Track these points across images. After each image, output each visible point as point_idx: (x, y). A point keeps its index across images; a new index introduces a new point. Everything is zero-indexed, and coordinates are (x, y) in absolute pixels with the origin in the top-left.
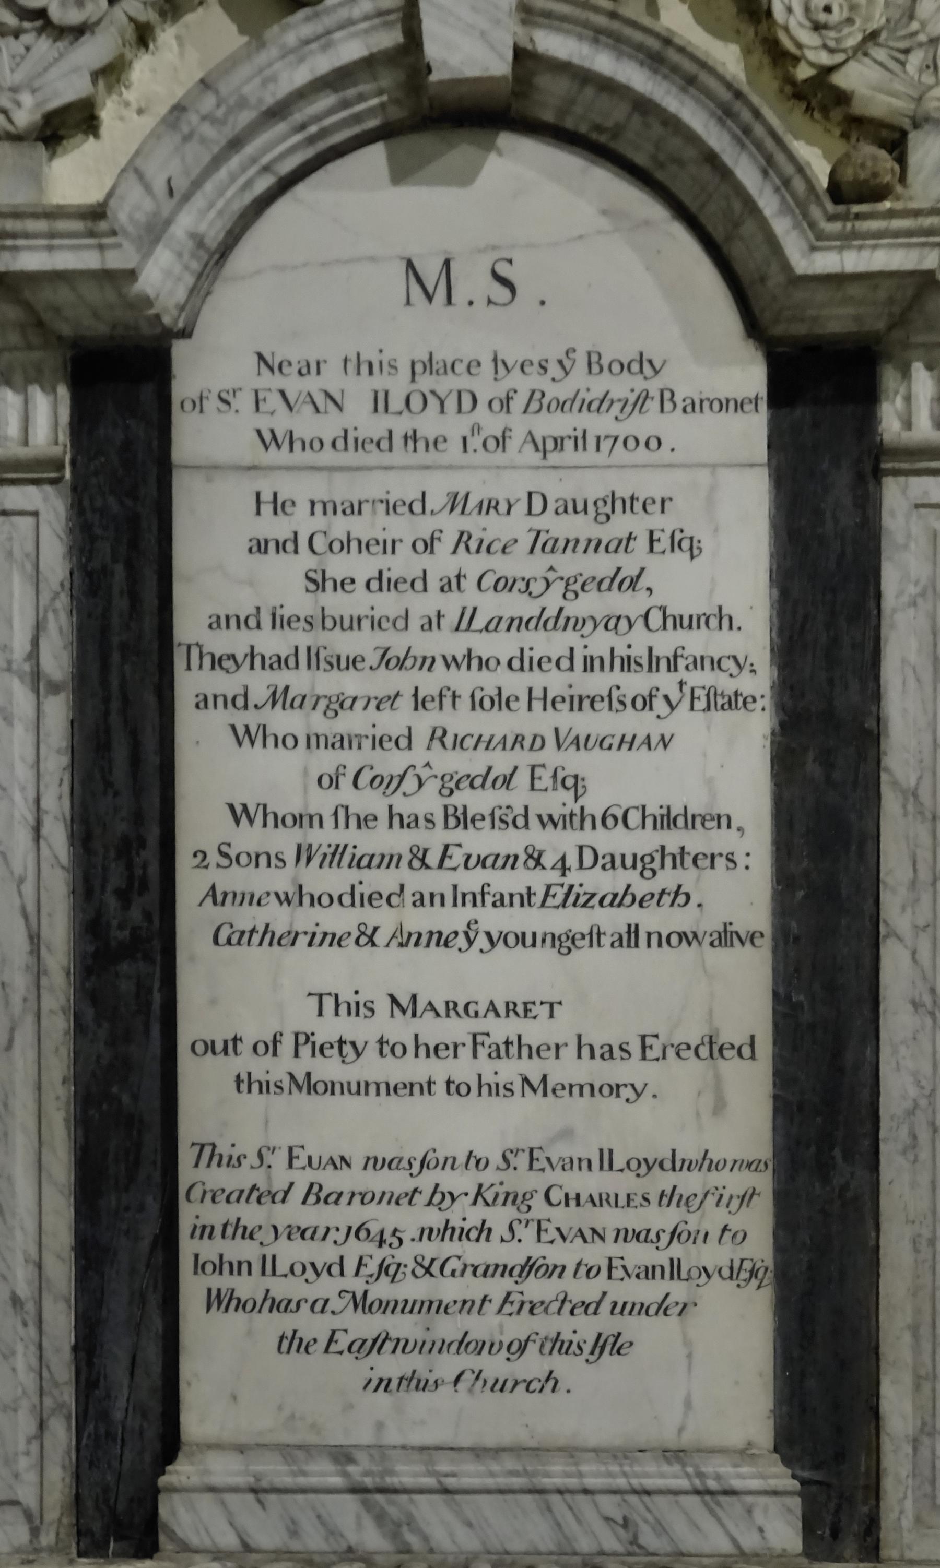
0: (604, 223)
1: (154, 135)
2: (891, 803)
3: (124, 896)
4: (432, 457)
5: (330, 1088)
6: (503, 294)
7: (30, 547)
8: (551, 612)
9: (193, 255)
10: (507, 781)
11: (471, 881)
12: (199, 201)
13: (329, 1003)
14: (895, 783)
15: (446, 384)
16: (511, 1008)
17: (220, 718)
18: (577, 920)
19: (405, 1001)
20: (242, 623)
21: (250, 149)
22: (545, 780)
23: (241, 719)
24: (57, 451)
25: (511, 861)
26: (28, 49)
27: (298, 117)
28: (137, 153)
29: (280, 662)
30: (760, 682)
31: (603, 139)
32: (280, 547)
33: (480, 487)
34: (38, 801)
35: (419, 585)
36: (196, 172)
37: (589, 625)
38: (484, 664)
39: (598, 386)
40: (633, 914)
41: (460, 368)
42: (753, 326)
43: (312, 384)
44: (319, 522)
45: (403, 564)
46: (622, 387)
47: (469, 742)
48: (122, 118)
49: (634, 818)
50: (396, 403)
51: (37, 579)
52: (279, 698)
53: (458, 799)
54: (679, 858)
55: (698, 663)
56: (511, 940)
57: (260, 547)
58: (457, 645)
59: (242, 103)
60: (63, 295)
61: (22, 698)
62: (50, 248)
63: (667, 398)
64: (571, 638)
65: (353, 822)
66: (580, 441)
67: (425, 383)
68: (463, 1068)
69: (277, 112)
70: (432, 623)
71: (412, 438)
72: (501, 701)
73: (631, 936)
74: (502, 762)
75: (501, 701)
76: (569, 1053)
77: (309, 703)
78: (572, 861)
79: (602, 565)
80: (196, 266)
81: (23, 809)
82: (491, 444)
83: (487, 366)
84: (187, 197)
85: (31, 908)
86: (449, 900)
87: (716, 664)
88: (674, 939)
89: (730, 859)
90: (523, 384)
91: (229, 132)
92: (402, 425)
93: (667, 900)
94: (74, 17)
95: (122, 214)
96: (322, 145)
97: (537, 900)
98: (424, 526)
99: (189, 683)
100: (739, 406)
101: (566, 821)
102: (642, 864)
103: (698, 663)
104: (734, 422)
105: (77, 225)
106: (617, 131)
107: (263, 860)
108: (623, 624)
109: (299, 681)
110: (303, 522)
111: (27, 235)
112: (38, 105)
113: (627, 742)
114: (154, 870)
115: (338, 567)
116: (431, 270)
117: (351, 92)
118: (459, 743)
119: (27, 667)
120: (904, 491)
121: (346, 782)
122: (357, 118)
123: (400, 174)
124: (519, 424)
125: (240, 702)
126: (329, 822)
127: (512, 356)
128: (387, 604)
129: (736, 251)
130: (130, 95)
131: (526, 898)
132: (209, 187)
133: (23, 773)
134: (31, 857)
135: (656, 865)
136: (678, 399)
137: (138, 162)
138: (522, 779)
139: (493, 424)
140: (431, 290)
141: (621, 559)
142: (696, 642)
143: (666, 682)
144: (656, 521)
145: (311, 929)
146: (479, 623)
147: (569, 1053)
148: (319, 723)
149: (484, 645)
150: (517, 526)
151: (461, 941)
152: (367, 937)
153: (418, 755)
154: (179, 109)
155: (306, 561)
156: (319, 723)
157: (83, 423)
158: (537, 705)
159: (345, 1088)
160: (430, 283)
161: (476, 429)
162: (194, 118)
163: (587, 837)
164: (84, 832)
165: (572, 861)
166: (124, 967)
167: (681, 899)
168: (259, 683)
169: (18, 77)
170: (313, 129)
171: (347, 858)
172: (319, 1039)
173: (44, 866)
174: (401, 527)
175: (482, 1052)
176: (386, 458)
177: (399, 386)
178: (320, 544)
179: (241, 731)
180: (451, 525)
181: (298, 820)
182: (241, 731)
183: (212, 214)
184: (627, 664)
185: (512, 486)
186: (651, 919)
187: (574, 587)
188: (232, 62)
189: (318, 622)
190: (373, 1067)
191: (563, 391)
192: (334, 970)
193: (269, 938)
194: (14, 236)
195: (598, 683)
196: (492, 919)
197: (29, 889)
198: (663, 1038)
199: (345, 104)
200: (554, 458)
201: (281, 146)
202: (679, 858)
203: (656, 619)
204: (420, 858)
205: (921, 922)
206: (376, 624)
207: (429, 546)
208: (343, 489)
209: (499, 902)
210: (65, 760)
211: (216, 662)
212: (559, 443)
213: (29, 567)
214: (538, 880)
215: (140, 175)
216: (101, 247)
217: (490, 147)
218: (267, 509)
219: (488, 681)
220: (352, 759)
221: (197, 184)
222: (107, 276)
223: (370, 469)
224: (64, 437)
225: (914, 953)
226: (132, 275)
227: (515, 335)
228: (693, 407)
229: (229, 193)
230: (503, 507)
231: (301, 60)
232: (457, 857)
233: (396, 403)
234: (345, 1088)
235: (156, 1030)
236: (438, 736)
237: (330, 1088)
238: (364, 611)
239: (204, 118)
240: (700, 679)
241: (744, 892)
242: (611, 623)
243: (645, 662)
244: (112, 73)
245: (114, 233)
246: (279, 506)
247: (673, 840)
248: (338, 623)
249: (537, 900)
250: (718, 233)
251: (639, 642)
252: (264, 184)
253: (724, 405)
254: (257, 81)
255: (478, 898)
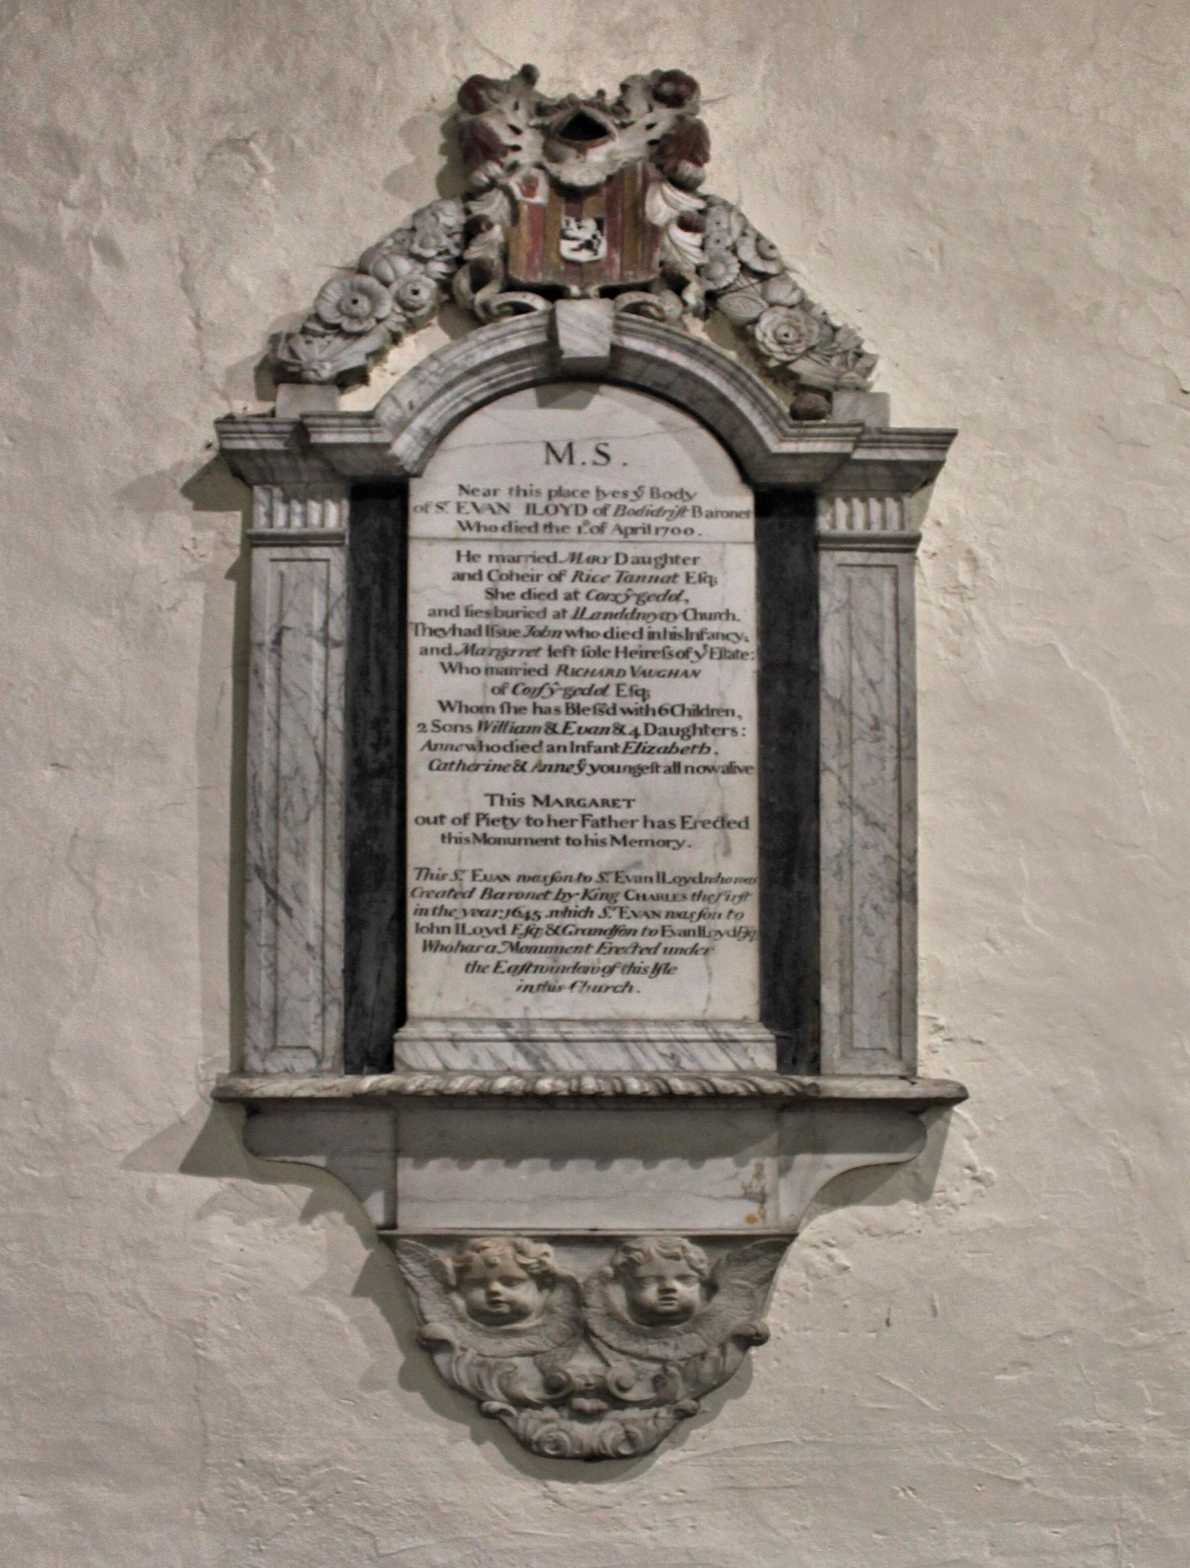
0: (660, 428)
1: (403, 381)
2: (825, 706)
3: (376, 747)
4: (560, 536)
5: (498, 841)
6: (602, 460)
7: (324, 576)
8: (629, 611)
9: (423, 438)
10: (603, 691)
11: (582, 740)
12: (427, 413)
13: (497, 800)
14: (828, 697)
15: (568, 502)
16: (605, 803)
17: (433, 660)
18: (645, 760)
19: (542, 798)
20: (448, 613)
21: (458, 389)
22: (626, 691)
23: (447, 660)
24: (340, 530)
25: (605, 731)
26: (329, 342)
27: (485, 375)
28: (393, 388)
29: (470, 633)
30: (751, 646)
31: (660, 389)
32: (471, 577)
33: (587, 550)
34: (326, 700)
35: (552, 596)
36: (426, 398)
37: (651, 618)
38: (590, 635)
39: (657, 504)
40: (677, 757)
41: (577, 494)
42: (746, 477)
43: (492, 500)
44: (494, 565)
45: (543, 586)
46: (670, 505)
47: (581, 673)
48: (382, 377)
49: (678, 710)
50: (540, 510)
51: (327, 591)
52: (469, 650)
53: (575, 700)
54: (704, 730)
55: (715, 636)
56: (605, 769)
57: (459, 577)
58: (574, 625)
59: (454, 367)
60: (348, 455)
61: (318, 650)
62: (341, 432)
63: (697, 511)
64: (641, 623)
65: (512, 711)
66: (647, 529)
67: (557, 501)
68: (577, 832)
69: (473, 372)
70: (559, 615)
71: (549, 527)
72: (600, 653)
73: (676, 768)
74: (600, 683)
75: (600, 653)
76: (639, 825)
77: (487, 653)
78: (641, 730)
79: (660, 588)
80: (424, 443)
81: (317, 703)
82: (595, 530)
83: (593, 494)
84: (420, 410)
85: (321, 752)
86: (569, 749)
87: (726, 637)
88: (701, 770)
89: (734, 731)
90: (614, 502)
91: (446, 380)
92: (543, 521)
93: (697, 750)
94: (357, 327)
95: (383, 417)
96: (497, 390)
97: (621, 749)
98: (556, 568)
99: (416, 643)
100: (738, 515)
101: (638, 712)
102: (683, 733)
103: (715, 636)
104: (736, 523)
105: (358, 421)
106: (668, 386)
107: (459, 729)
108: (671, 617)
109: (481, 642)
110: (485, 566)
111: (327, 426)
112: (333, 369)
113: (674, 674)
114: (394, 734)
115: (505, 587)
116: (561, 448)
117: (517, 364)
118: (575, 673)
119: (321, 634)
120: (832, 558)
121: (508, 691)
122: (519, 377)
123: (543, 403)
124: (611, 521)
125: (447, 651)
126: (498, 711)
127: (608, 487)
128: (534, 605)
129: (737, 443)
130: (386, 366)
131: (614, 749)
132: (433, 406)
133: (317, 685)
134: (321, 727)
135: (691, 733)
136: (703, 510)
137: (394, 392)
138: (612, 691)
139: (597, 521)
140: (560, 456)
141: (670, 586)
142: (713, 626)
143: (696, 645)
144: (690, 568)
145: (486, 761)
146: (588, 614)
147: (639, 825)
148: (492, 662)
149: (590, 626)
150: (611, 569)
151: (576, 770)
152: (521, 767)
153: (551, 678)
154: (417, 369)
155: (486, 584)
156: (492, 662)
157: (356, 518)
158: (621, 655)
159: (507, 841)
160: (560, 454)
161: (586, 523)
162: (426, 373)
163: (649, 719)
164: (353, 715)
165: (641, 730)
166: (376, 782)
167: (705, 750)
168: (458, 643)
169: (324, 355)
170: (494, 381)
171: (509, 728)
172: (492, 817)
173: (329, 733)
174: (542, 569)
175: (588, 824)
176: (534, 536)
177: (541, 502)
178: (494, 576)
179: (447, 666)
180: (571, 568)
181: (480, 709)
182: (447, 666)
183: (435, 419)
184: (674, 636)
185: (609, 550)
186: (686, 760)
187: (642, 599)
188: (446, 349)
189: (493, 614)
190: (523, 831)
191: (638, 505)
192: (500, 783)
193: (462, 766)
194: (319, 426)
195: (657, 645)
196: (593, 759)
197: (320, 742)
198: (695, 817)
199: (512, 370)
200: (631, 537)
201: (475, 388)
202: (704, 730)
203: (690, 615)
204: (551, 729)
205: (844, 763)
206: (527, 615)
207: (559, 577)
208: (508, 550)
209: (599, 750)
210: (342, 679)
211: (433, 632)
212: (634, 530)
213: (323, 587)
214: (621, 740)
215: (395, 400)
216: (371, 432)
217: (595, 392)
218: (464, 559)
219: (593, 643)
220: (512, 680)
221: (426, 404)
222: (373, 446)
223: (524, 540)
224: (345, 524)
225: (839, 778)
226: (388, 446)
227: (611, 479)
228: (711, 515)
229: (445, 410)
230: (602, 560)
231: (488, 348)
232: (574, 728)
233: (540, 510)
234: (507, 841)
235: (394, 813)
236: (563, 669)
237: (498, 841)
238: (519, 608)
239: (432, 373)
240: (713, 643)
241: (743, 746)
242: (665, 616)
243: (684, 635)
244: (378, 355)
245: (378, 425)
246: (471, 558)
247: (700, 721)
248: (505, 614)
249: (621, 749)
250: (725, 433)
251: (681, 625)
252: (464, 406)
253: (729, 514)
254: (463, 356)
255: (586, 748)
